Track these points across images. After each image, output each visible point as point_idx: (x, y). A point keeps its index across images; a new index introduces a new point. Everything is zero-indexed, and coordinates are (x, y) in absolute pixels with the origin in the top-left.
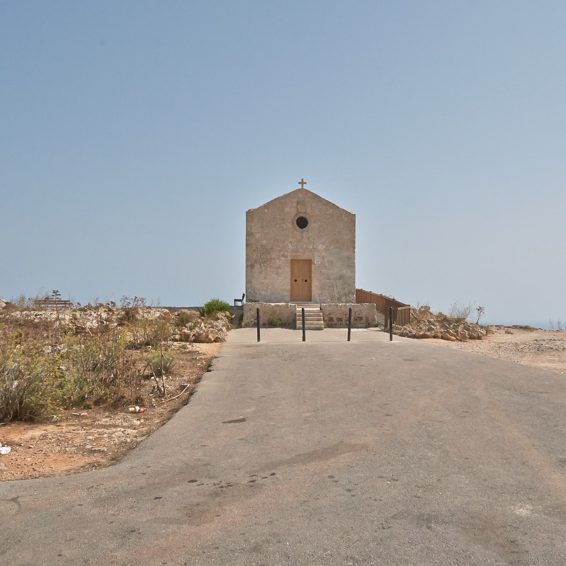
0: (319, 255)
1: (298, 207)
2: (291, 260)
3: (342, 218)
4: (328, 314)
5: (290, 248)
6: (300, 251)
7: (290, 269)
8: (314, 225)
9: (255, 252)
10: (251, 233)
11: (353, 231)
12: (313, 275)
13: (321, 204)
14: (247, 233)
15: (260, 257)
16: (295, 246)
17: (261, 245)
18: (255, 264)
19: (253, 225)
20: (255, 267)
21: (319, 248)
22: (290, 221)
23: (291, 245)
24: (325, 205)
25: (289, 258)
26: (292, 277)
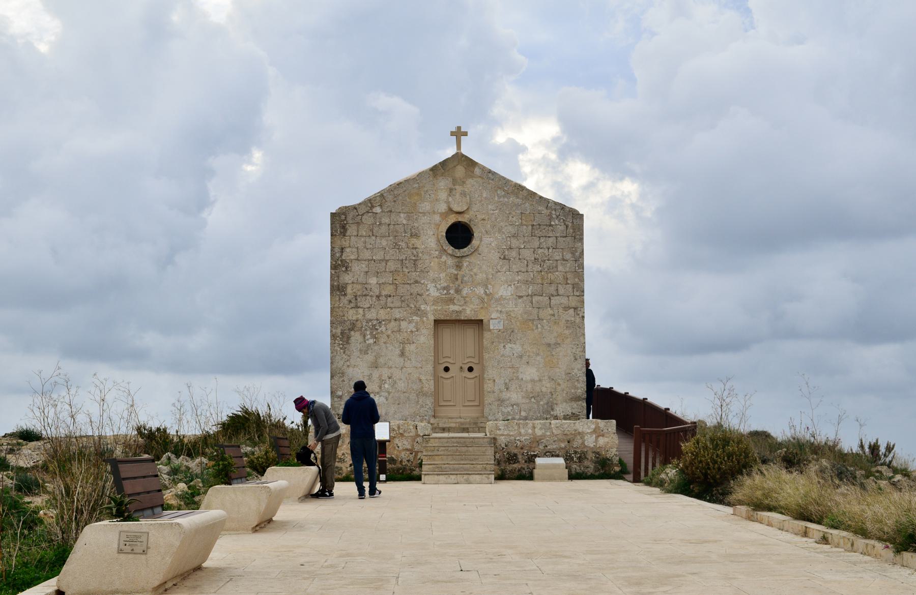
0: (500, 309)
1: (450, 199)
2: (435, 320)
3: (553, 223)
4: (503, 446)
5: (432, 295)
7: (432, 342)
8: (487, 240)
9: (352, 305)
10: (341, 261)
11: (577, 254)
12: (486, 356)
13: (503, 193)
14: (334, 263)
15: (364, 315)
16: (444, 288)
17: (367, 289)
18: (352, 333)
19: (346, 244)
20: (351, 338)
22: (432, 233)
23: (436, 287)
25: (432, 318)
26: (436, 362)
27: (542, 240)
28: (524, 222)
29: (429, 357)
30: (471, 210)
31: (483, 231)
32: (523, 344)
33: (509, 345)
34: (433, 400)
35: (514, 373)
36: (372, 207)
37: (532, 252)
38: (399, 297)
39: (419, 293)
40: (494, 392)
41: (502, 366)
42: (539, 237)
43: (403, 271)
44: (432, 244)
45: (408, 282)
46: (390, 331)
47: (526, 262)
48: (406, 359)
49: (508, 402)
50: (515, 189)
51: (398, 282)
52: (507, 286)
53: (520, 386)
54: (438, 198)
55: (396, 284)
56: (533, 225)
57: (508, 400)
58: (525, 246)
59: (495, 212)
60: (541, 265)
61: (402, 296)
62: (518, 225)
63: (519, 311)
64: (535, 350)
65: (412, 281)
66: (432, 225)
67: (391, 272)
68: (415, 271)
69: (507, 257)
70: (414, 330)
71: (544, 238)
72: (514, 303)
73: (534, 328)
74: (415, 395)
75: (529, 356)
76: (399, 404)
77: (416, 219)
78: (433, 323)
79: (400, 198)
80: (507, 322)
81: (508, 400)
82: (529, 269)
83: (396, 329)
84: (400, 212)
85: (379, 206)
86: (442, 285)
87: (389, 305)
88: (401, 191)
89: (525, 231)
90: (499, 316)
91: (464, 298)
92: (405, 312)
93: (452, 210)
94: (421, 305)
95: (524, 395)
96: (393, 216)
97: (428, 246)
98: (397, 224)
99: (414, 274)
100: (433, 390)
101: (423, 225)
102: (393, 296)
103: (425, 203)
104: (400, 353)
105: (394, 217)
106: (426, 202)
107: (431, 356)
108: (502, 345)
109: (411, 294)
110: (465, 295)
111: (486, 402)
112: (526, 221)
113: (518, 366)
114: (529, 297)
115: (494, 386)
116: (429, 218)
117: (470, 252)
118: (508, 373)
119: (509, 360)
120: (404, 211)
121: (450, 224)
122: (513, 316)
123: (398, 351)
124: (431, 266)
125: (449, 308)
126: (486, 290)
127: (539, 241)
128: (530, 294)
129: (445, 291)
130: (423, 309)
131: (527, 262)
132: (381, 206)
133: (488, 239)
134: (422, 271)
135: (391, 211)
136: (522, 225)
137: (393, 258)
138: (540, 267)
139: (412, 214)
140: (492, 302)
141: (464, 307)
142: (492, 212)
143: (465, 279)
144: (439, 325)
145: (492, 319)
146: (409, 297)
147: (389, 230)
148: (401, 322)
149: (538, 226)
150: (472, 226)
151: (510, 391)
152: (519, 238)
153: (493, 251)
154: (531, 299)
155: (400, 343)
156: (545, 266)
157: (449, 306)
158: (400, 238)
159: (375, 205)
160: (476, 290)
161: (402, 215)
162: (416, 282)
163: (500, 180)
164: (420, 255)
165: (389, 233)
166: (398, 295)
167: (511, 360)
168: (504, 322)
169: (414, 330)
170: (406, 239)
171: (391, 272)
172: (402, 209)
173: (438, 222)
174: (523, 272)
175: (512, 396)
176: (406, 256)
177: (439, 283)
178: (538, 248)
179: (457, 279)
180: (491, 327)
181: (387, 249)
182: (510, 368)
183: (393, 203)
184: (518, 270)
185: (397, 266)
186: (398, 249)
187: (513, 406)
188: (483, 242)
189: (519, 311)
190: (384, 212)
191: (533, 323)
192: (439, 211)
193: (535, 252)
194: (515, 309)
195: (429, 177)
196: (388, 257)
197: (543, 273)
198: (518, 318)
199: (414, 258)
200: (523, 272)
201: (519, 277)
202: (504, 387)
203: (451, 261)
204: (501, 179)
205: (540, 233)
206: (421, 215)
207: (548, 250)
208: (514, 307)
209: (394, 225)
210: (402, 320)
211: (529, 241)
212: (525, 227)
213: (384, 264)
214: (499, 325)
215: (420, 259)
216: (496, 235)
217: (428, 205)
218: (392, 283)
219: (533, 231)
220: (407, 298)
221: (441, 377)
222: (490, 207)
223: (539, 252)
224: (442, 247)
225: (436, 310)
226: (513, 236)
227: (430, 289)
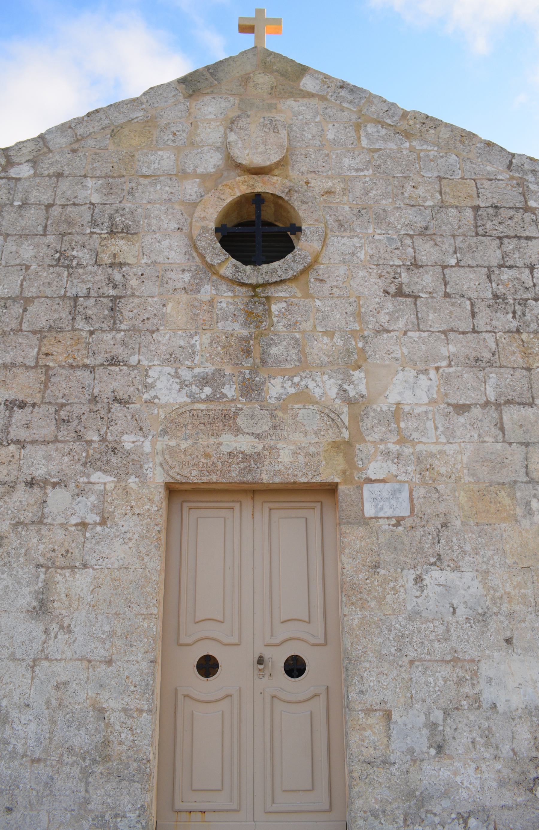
0: (394, 448)
1: (232, 137)
6: (239, 421)
13: (383, 132)
16: (205, 381)
21: (393, 398)
22: (174, 225)
23: (177, 375)
24: (408, 135)
27: (509, 246)
28: (449, 200)
29: (140, 618)
30: (293, 169)
31: (331, 221)
32: (487, 572)
33: (436, 573)
34: (150, 797)
35: (460, 682)
36: (10, 163)
37: (484, 277)
38: (52, 409)
39: (121, 395)
40: (386, 762)
41: (413, 654)
42: (500, 238)
43: (74, 330)
44: (172, 254)
45: (87, 361)
46: (8, 523)
47: (468, 302)
48: (54, 628)
49: (446, 803)
50: (415, 124)
51: (55, 361)
52: (414, 373)
53: (488, 734)
54: (198, 139)
55: (48, 367)
56: (476, 208)
57: (445, 794)
58: (459, 261)
59: (362, 174)
60: (514, 312)
61: (63, 405)
62: (433, 207)
63: (461, 452)
64: (529, 592)
65: (100, 359)
66: (177, 207)
67: (34, 332)
68: (112, 330)
69: (406, 290)
70: (92, 518)
71: (515, 241)
72: (441, 429)
73: (519, 511)
74: (76, 771)
75: (510, 615)
76: (9, 810)
77: (131, 192)
78: (160, 495)
79: (91, 142)
80: (422, 491)
81: (445, 794)
82: (481, 322)
83: (28, 516)
84: (85, 176)
85: (28, 161)
86: (196, 371)
87: (13, 435)
88: (96, 126)
89: (455, 222)
90: (393, 469)
91: (272, 411)
92: (66, 459)
93: (239, 166)
94: (123, 433)
95: (505, 772)
96: (64, 185)
97: (161, 259)
98: (74, 204)
99: (108, 337)
100: (152, 753)
101: (149, 206)
102: (34, 405)
103: (160, 153)
104: (35, 604)
105: (64, 188)
106: (160, 150)
107: (146, 617)
108: (412, 575)
109: (94, 399)
110: (273, 401)
111: (359, 803)
112: (454, 197)
113: (474, 653)
114: (493, 412)
115: (389, 737)
116: (167, 188)
117: (290, 274)
118: (441, 682)
119: (441, 629)
120: (98, 173)
121: (229, 199)
122: (443, 470)
123: (28, 598)
124: (164, 315)
125: (221, 444)
126: (345, 386)
127: (500, 247)
128: (492, 399)
129: (208, 390)
130: (128, 446)
131: (472, 305)
132: (34, 162)
133: (345, 240)
134: (134, 329)
135: (59, 175)
136: (447, 207)
137: (49, 293)
138: (514, 317)
139: (119, 180)
140: (367, 423)
141: (269, 442)
142: (354, 173)
143: (274, 350)
144: (185, 505)
145: (369, 481)
146: (85, 409)
147: (47, 219)
148: (49, 488)
149: (491, 211)
150: (296, 204)
151: (451, 757)
152: (439, 239)
153: (361, 274)
154: (496, 415)
155: (38, 566)
156: (528, 317)
157: (218, 436)
158: (77, 238)
159: (15, 160)
160: (312, 385)
161: (90, 183)
162: (114, 361)
163: (371, 102)
164: (134, 283)
165: (46, 227)
166: (50, 403)
167: (448, 630)
168: (411, 491)
169: (92, 518)
170: (96, 240)
171: (34, 332)
172: (94, 169)
173: (194, 197)
174: (464, 333)
175: (458, 779)
176: (89, 285)
177: (188, 363)
178: (500, 266)
179: (248, 352)
180: (369, 510)
181: (32, 268)
182: (448, 662)
183: (69, 156)
184: (444, 327)
185: (56, 316)
186: (68, 267)
187: (466, 822)
188: (331, 249)
189: (461, 452)
190: (42, 176)
191: (512, 496)
192: (200, 170)
193: (493, 277)
194: (450, 449)
195: (174, 96)
196: (33, 290)
197: (524, 336)
198: (460, 478)
199: (112, 292)
200: (464, 333)
201: (452, 348)
202: (425, 742)
203: (230, 300)
204: (375, 101)
205: (501, 228)
206: (146, 181)
207: (532, 273)
208: (443, 439)
209: (63, 206)
210: (54, 485)
211: (469, 247)
212: (454, 211)
213: (17, 310)
214: (393, 502)
215: (133, 295)
216: (370, 231)
217: (169, 158)
218: (33, 364)
219: (480, 223)
220: (77, 410)
221: (185, 696)
222: (346, 161)
223: (505, 277)
224: (203, 257)
225: (172, 451)
226: (420, 235)
227: (159, 385)
